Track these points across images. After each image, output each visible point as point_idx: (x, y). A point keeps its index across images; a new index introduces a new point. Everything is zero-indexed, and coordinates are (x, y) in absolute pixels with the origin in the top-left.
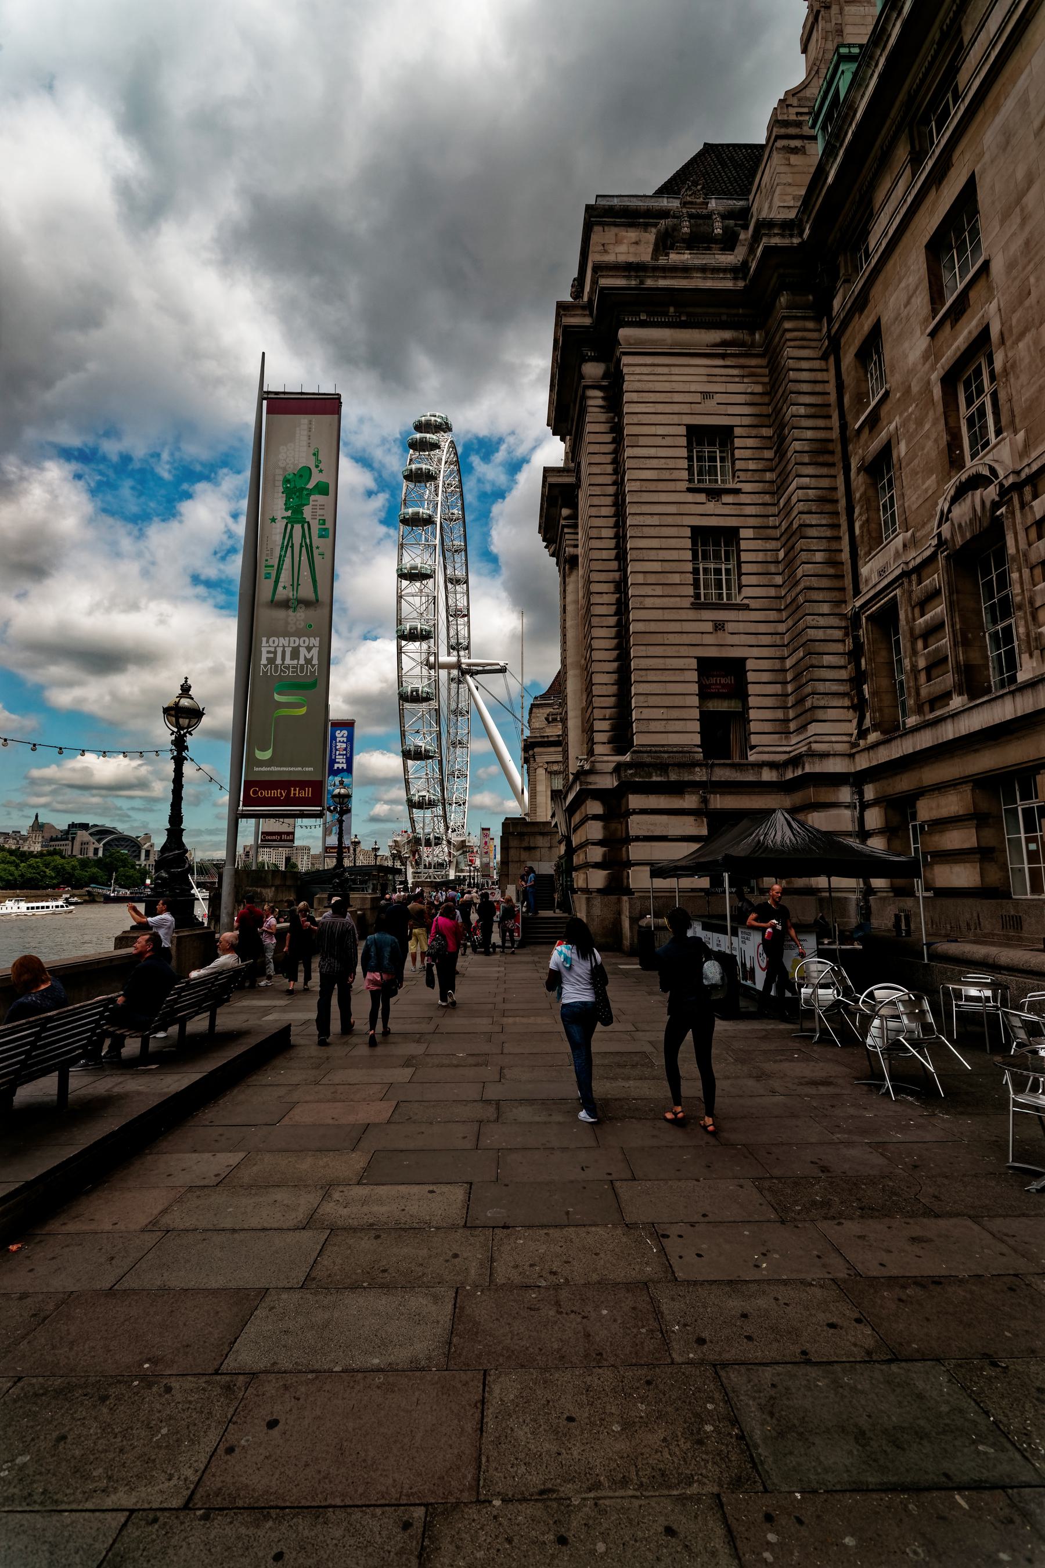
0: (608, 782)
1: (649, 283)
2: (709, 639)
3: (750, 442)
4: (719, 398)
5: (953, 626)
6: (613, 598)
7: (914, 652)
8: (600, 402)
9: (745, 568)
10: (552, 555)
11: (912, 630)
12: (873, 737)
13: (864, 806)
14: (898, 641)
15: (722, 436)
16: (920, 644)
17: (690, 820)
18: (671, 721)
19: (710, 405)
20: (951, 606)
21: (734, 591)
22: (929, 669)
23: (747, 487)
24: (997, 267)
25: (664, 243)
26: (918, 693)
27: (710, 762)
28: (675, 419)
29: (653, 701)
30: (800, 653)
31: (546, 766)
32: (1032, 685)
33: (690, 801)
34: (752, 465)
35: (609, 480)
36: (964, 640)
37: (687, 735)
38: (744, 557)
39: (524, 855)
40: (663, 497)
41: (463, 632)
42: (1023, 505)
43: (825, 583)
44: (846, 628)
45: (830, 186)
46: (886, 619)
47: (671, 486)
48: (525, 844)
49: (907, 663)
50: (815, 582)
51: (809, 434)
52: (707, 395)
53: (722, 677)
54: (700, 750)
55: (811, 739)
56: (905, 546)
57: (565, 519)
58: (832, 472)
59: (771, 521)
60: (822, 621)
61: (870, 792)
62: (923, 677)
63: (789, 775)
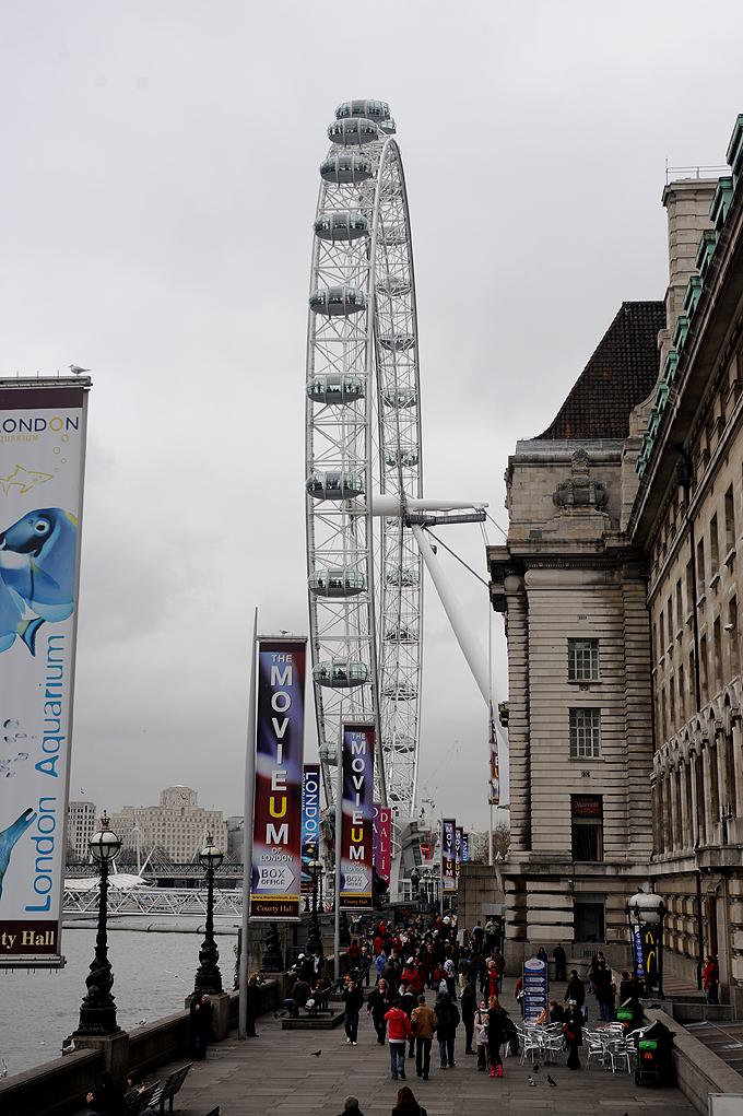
0: (516, 870)
1: (543, 550)
2: (578, 782)
3: (609, 650)
4: (590, 619)
23: (606, 680)
28: (561, 634)
33: (563, 886)
35: (522, 662)
37: (563, 843)
39: (480, 897)
40: (553, 688)
41: (410, 435)
43: (642, 757)
47: (557, 680)
50: (635, 756)
51: (636, 661)
52: (581, 617)
53: (586, 807)
59: (621, 704)
60: (639, 781)
63: (622, 873)
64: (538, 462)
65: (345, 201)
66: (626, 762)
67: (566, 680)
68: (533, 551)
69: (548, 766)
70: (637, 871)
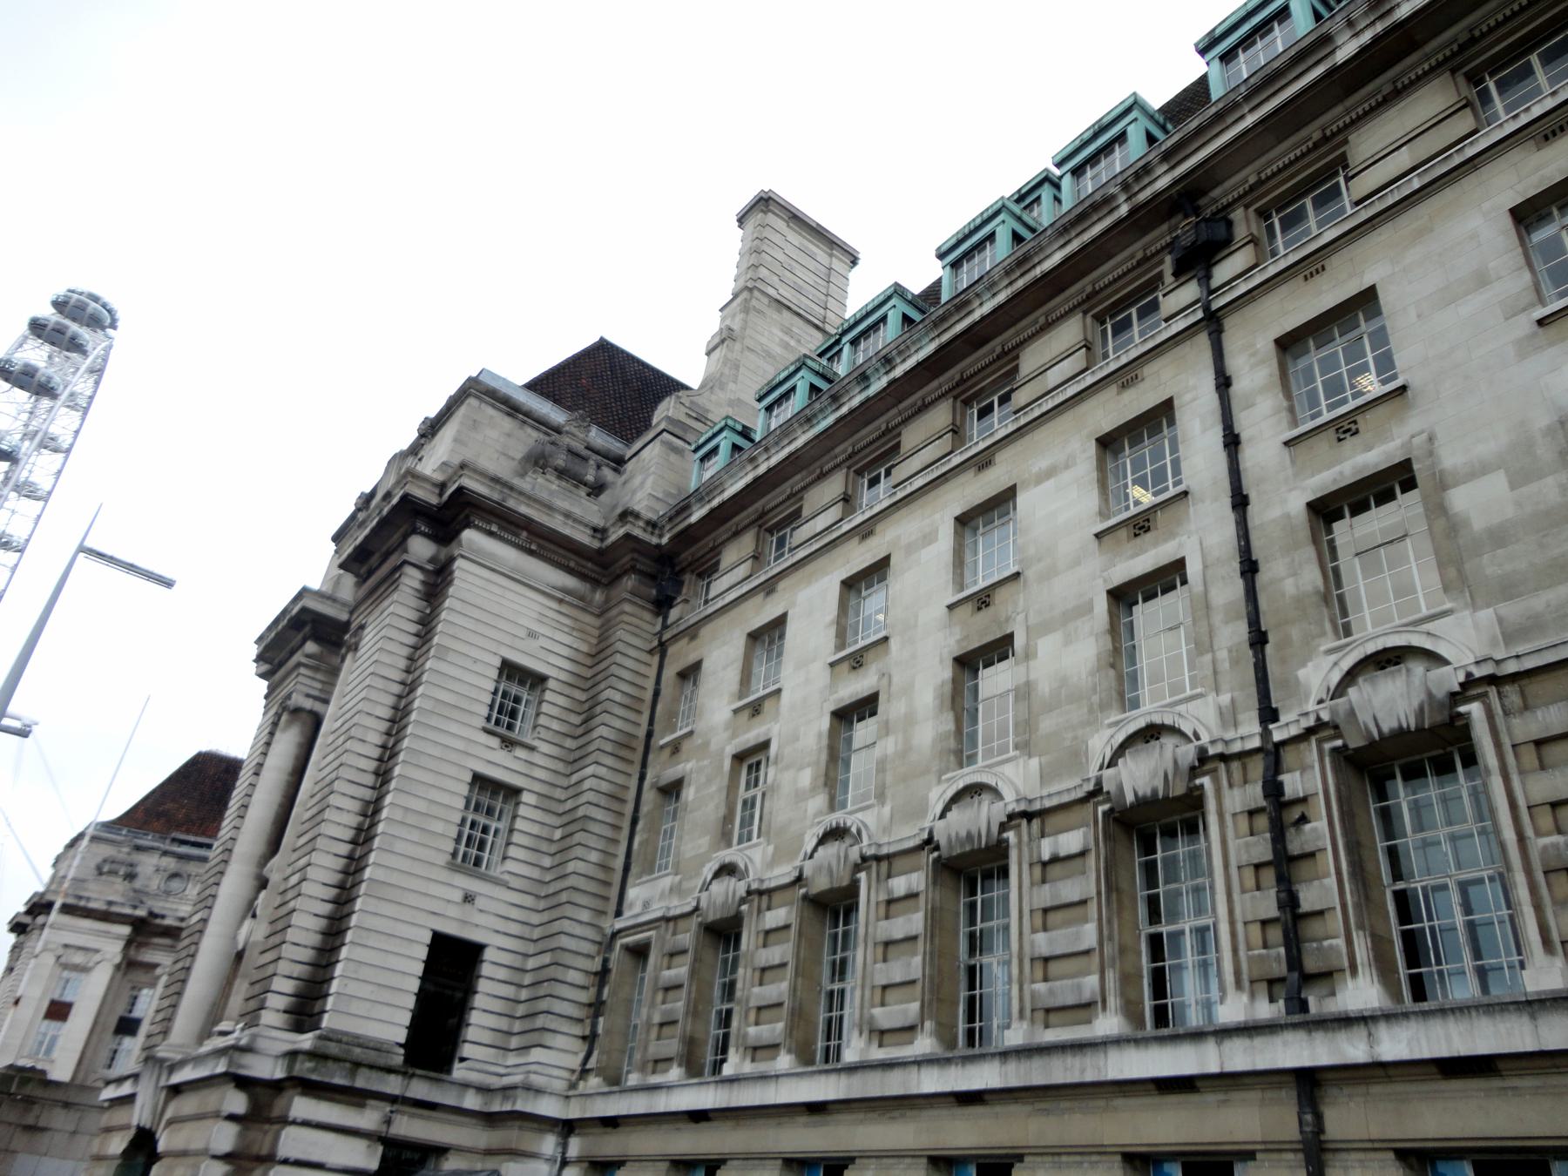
0: (266, 1068)
1: (511, 503)
2: (453, 911)
5: (689, 993)
6: (354, 820)
7: (653, 1005)
8: (417, 585)
9: (516, 838)
10: (262, 676)
11: (656, 979)
12: (594, 1082)
13: (565, 1163)
14: (642, 979)
15: (537, 681)
16: (660, 996)
17: (360, 1145)
18: (375, 1000)
19: (533, 645)
20: (693, 972)
21: (496, 857)
22: (662, 1025)
23: (544, 748)
24: (784, 694)
25: (537, 461)
26: (646, 1048)
27: (411, 1071)
28: (493, 647)
29: (365, 973)
30: (546, 959)
31: (60, 951)
32: (732, 1080)
33: (368, 1118)
34: (555, 726)
35: (398, 676)
36: (694, 1011)
37: (389, 1022)
38: (519, 824)
39: (20, 1140)
40: (454, 728)
42: (759, 911)
43: (592, 887)
44: (600, 943)
45: (691, 526)
46: (639, 953)
48: (30, 1120)
49: (644, 1011)
51: (618, 724)
52: (532, 634)
54: (402, 1051)
55: (533, 1067)
56: (671, 889)
57: (308, 656)
58: (629, 769)
59: (559, 794)
60: (579, 930)
61: (575, 1147)
62: (654, 1033)
63: (497, 1106)
64: (511, 408)
65: (37, 354)
66: (550, 898)
67: (481, 723)
68: (496, 496)
69: (405, 865)
70: (548, 1107)
